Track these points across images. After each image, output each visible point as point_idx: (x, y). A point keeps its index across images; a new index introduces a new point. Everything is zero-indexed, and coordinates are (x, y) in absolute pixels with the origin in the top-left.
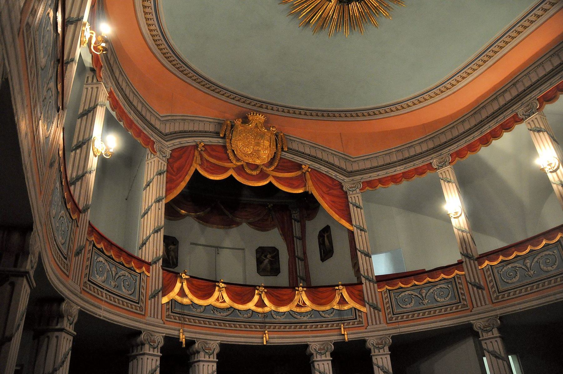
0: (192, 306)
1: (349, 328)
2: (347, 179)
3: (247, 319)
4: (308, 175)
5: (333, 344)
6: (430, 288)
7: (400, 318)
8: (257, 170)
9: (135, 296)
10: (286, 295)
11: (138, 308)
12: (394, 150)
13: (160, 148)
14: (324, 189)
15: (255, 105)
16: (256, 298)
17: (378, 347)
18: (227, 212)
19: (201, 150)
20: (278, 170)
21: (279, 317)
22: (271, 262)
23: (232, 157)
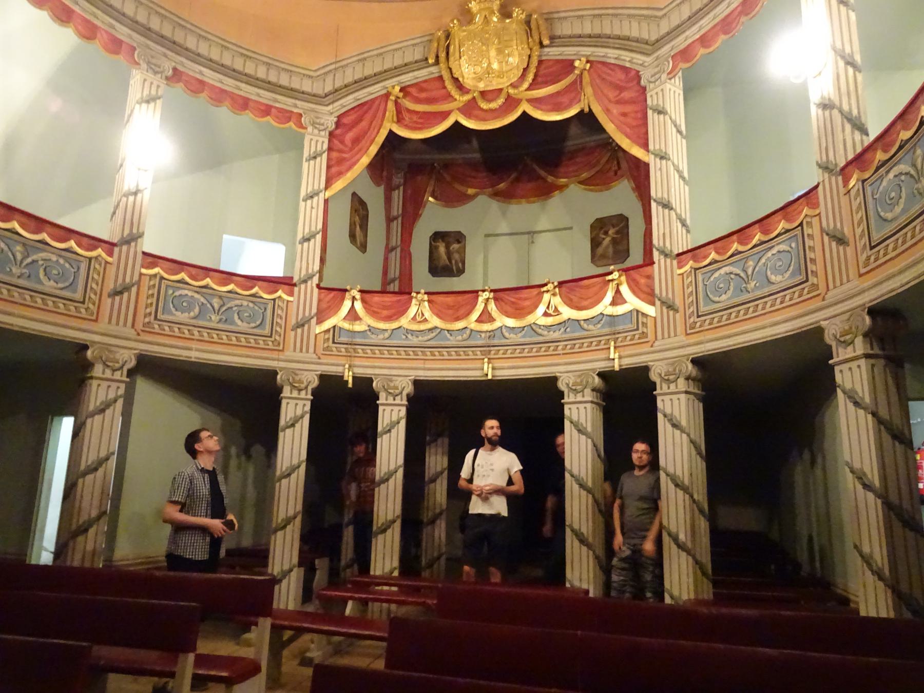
1: (625, 346)
2: (648, 60)
4: (586, 78)
9: (264, 329)
11: (270, 343)
14: (612, 94)
18: (542, 173)
21: (515, 336)
22: (614, 242)
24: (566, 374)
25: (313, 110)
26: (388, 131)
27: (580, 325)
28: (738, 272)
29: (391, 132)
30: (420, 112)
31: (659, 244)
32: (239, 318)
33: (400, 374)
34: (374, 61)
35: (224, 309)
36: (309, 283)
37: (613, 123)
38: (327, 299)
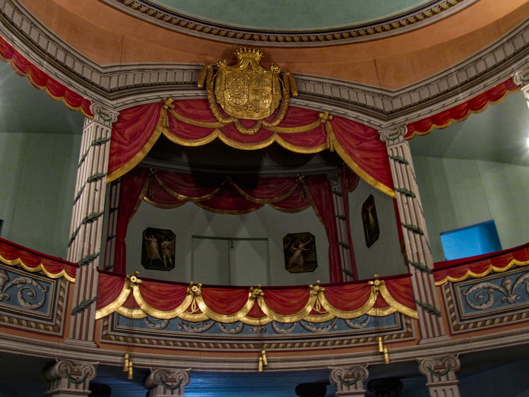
0: (147, 320)
2: (385, 124)
3: (236, 335)
4: (329, 126)
5: (367, 368)
6: (519, 275)
7: (471, 325)
8: (254, 128)
9: (46, 312)
10: (296, 297)
11: (50, 328)
12: (453, 70)
13: (100, 110)
14: (353, 142)
15: (242, 38)
16: (249, 304)
17: (438, 373)
18: (242, 192)
19: (169, 108)
20: (286, 125)
21: (285, 331)
22: (304, 253)
23: (217, 114)
24: (337, 368)
25: (100, 101)
26: (160, 133)
27: (346, 323)
28: (497, 287)
29: (162, 136)
30: (187, 124)
31: (414, 261)
32: (22, 298)
33: (178, 365)
34: (150, 74)
35: (9, 285)
36: (91, 264)
37: (357, 163)
38: (106, 285)
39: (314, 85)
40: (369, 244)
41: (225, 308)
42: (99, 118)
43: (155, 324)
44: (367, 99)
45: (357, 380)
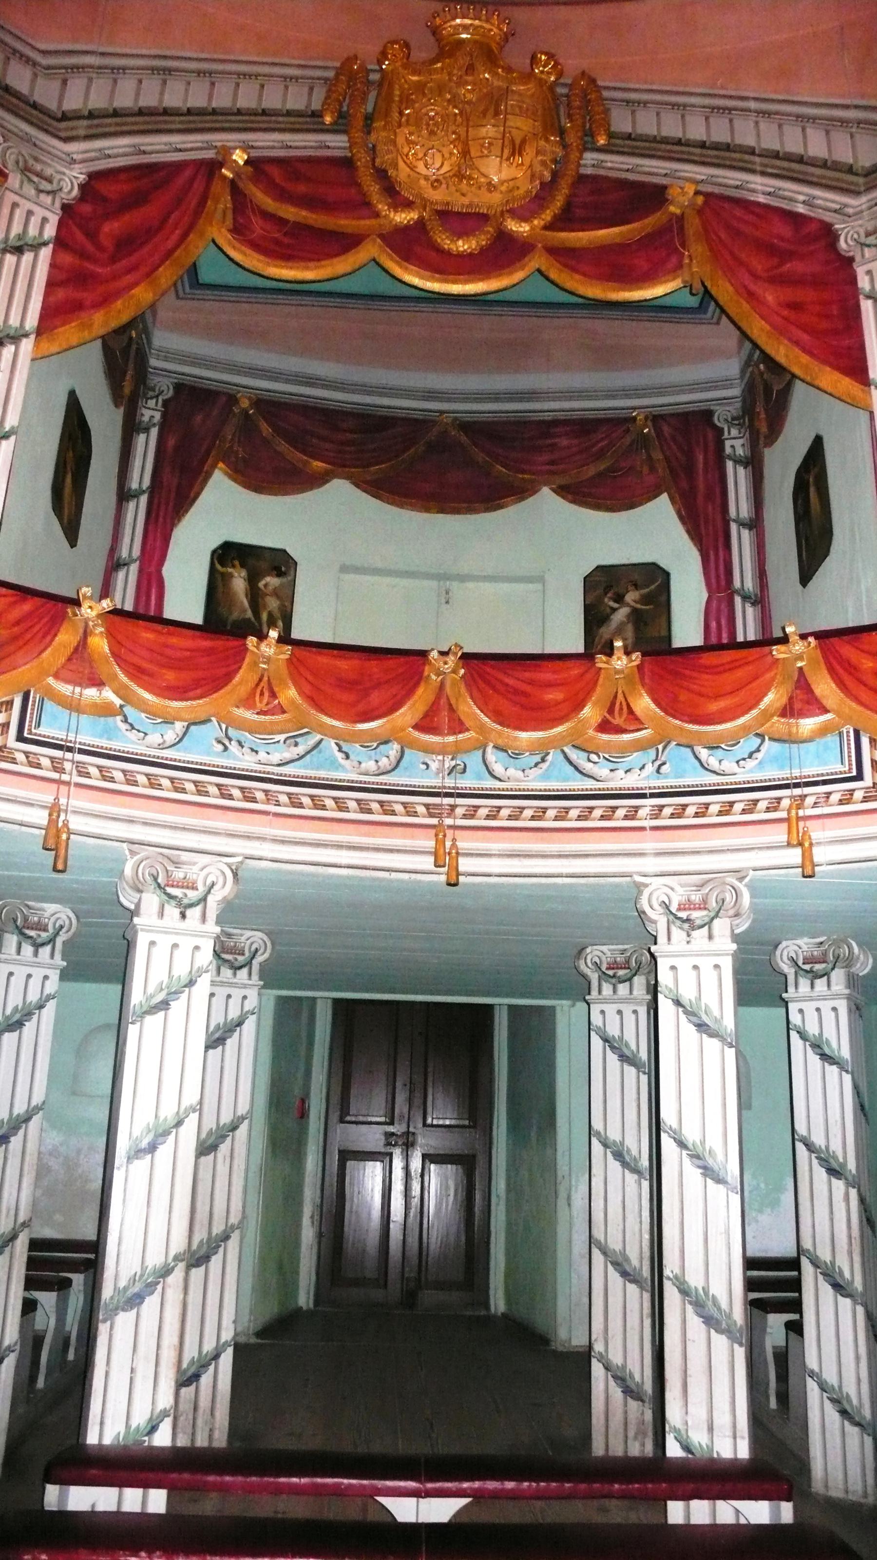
5: (746, 885)
13: (25, 161)
21: (521, 773)
22: (637, 618)
25: (27, 139)
39: (658, 114)
40: (805, 578)
41: (354, 705)
42: (22, 183)
43: (146, 734)
44: (809, 138)
45: (717, 916)
